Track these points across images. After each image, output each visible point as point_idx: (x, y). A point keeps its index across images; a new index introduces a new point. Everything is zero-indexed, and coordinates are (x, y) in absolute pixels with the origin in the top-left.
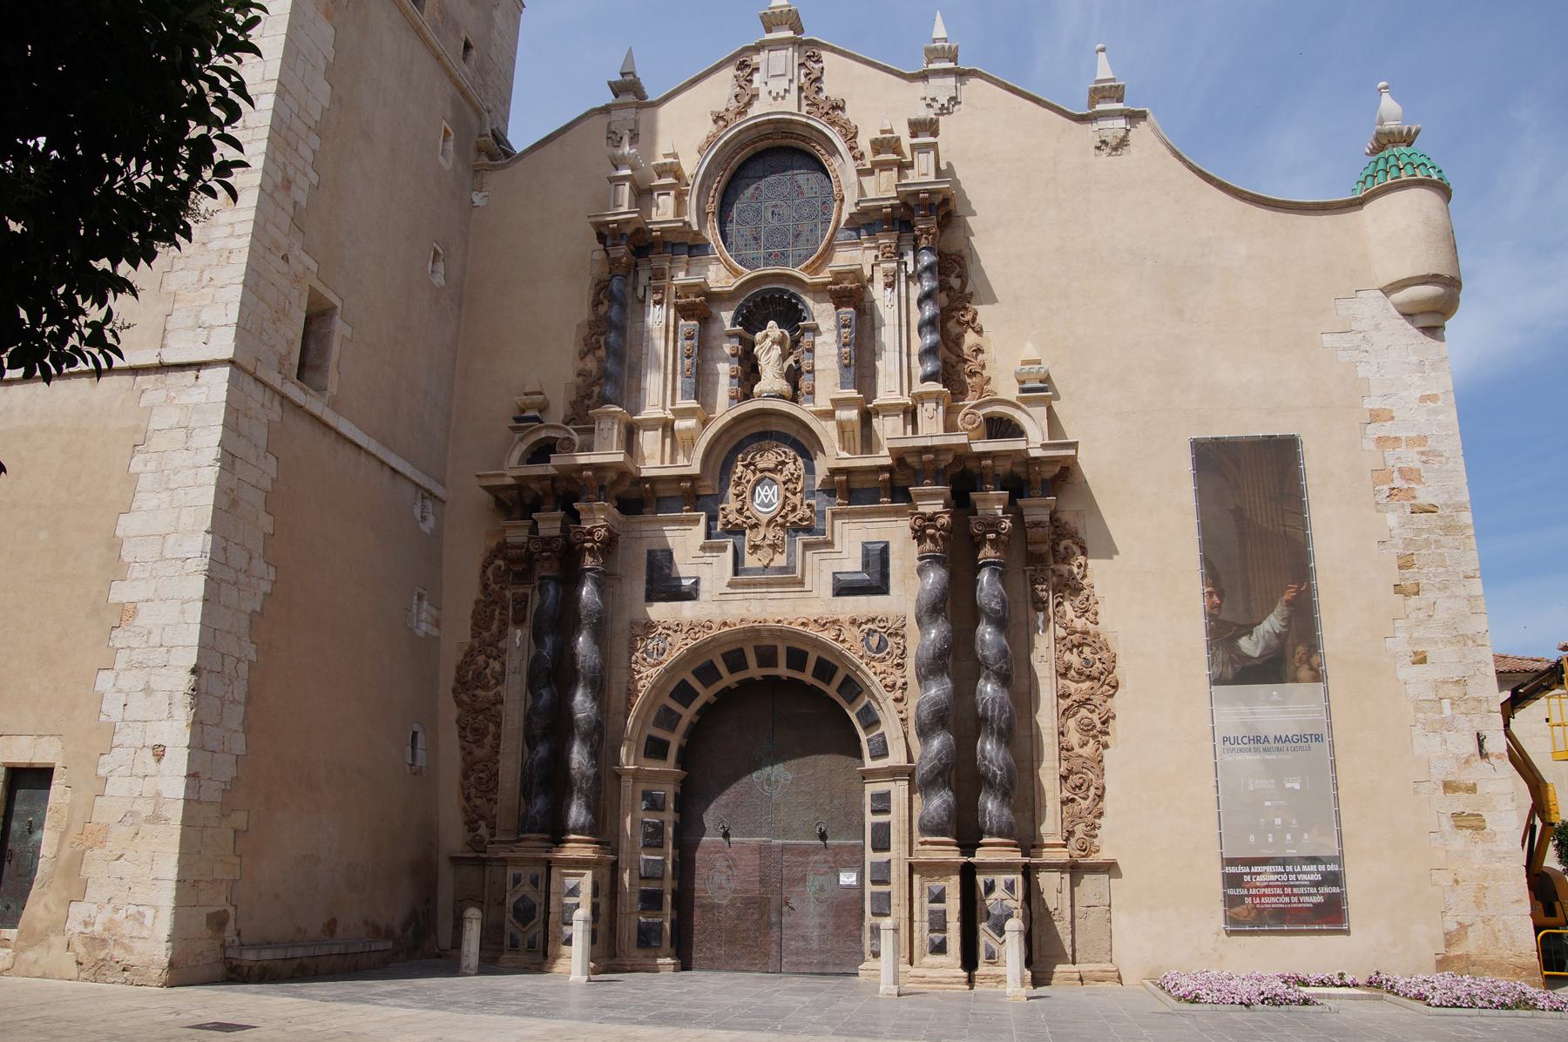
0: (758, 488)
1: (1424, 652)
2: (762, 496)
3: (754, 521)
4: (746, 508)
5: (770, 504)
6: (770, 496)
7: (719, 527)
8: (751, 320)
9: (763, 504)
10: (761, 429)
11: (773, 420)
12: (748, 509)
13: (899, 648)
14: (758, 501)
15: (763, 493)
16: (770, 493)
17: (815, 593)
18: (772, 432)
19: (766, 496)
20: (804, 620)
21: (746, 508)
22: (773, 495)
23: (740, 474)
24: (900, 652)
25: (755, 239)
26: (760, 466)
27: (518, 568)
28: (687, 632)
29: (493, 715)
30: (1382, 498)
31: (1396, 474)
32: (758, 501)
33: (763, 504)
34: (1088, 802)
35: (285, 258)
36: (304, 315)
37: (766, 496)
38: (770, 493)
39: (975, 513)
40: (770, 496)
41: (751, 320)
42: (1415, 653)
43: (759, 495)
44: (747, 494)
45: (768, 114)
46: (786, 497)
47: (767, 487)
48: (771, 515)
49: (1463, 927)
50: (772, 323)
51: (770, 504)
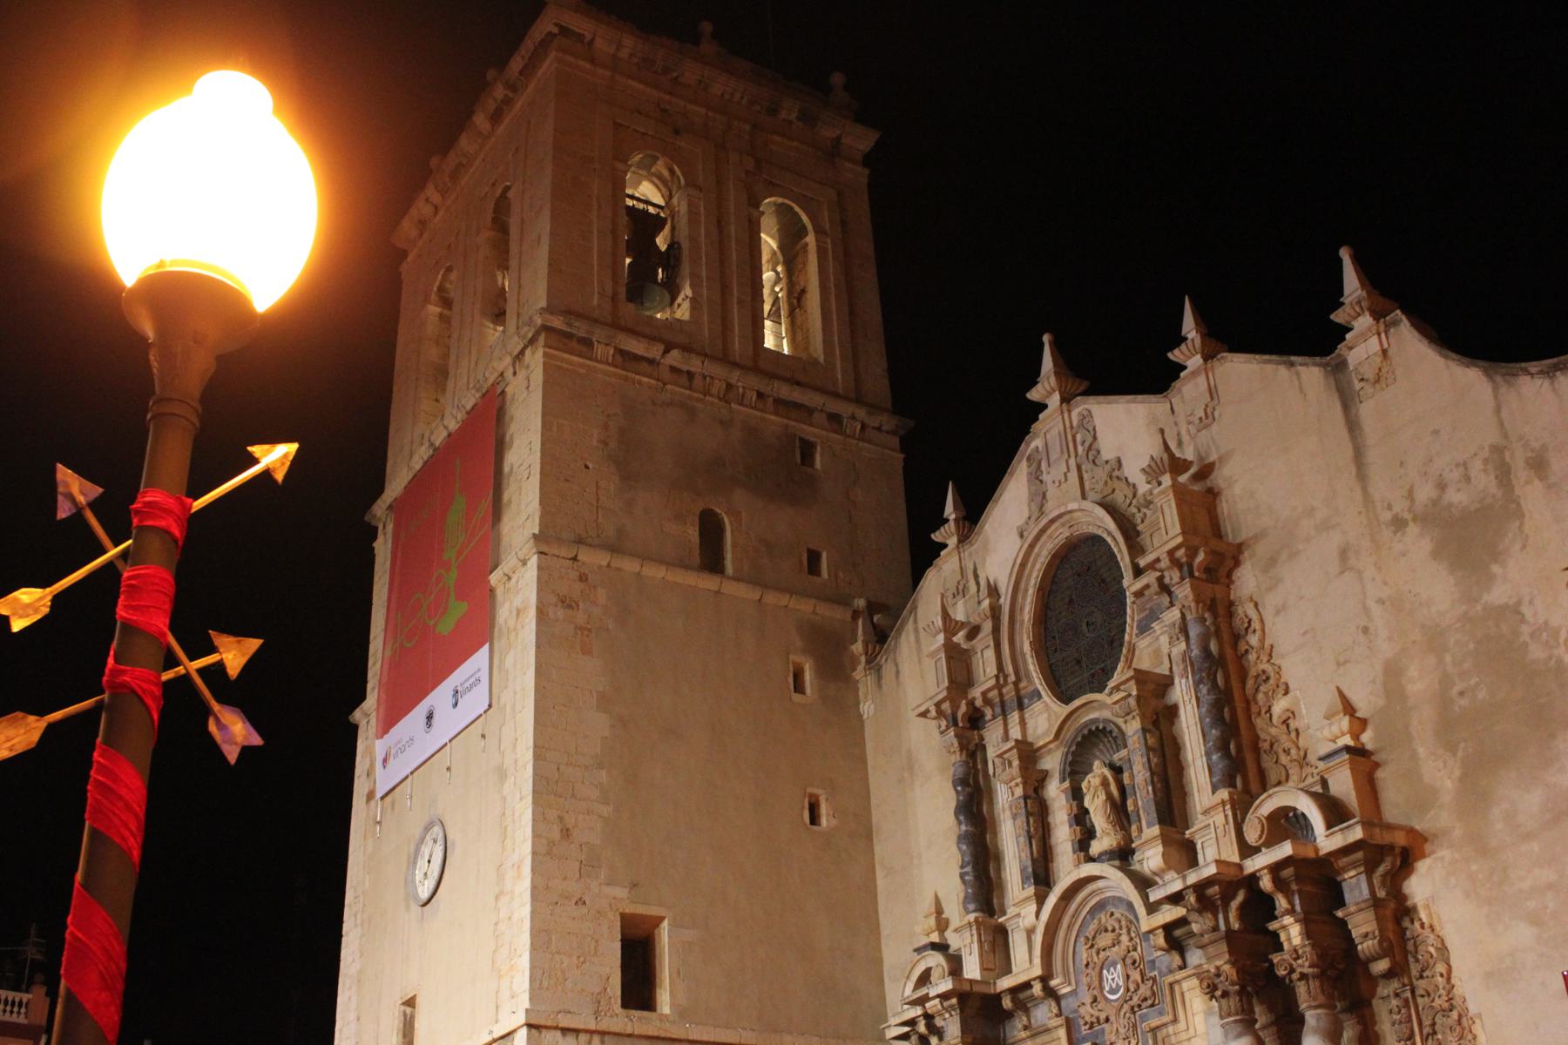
0: (1105, 972)
2: (1110, 980)
6: (1117, 979)
8: (1075, 771)
9: (1112, 991)
14: (1107, 988)
15: (1110, 977)
16: (1115, 975)
19: (1113, 979)
23: (1085, 962)
32: (1107, 988)
35: (581, 902)
36: (618, 945)
37: (1113, 979)
39: (1279, 947)
40: (1117, 979)
41: (1075, 771)
44: (1096, 983)
46: (1128, 976)
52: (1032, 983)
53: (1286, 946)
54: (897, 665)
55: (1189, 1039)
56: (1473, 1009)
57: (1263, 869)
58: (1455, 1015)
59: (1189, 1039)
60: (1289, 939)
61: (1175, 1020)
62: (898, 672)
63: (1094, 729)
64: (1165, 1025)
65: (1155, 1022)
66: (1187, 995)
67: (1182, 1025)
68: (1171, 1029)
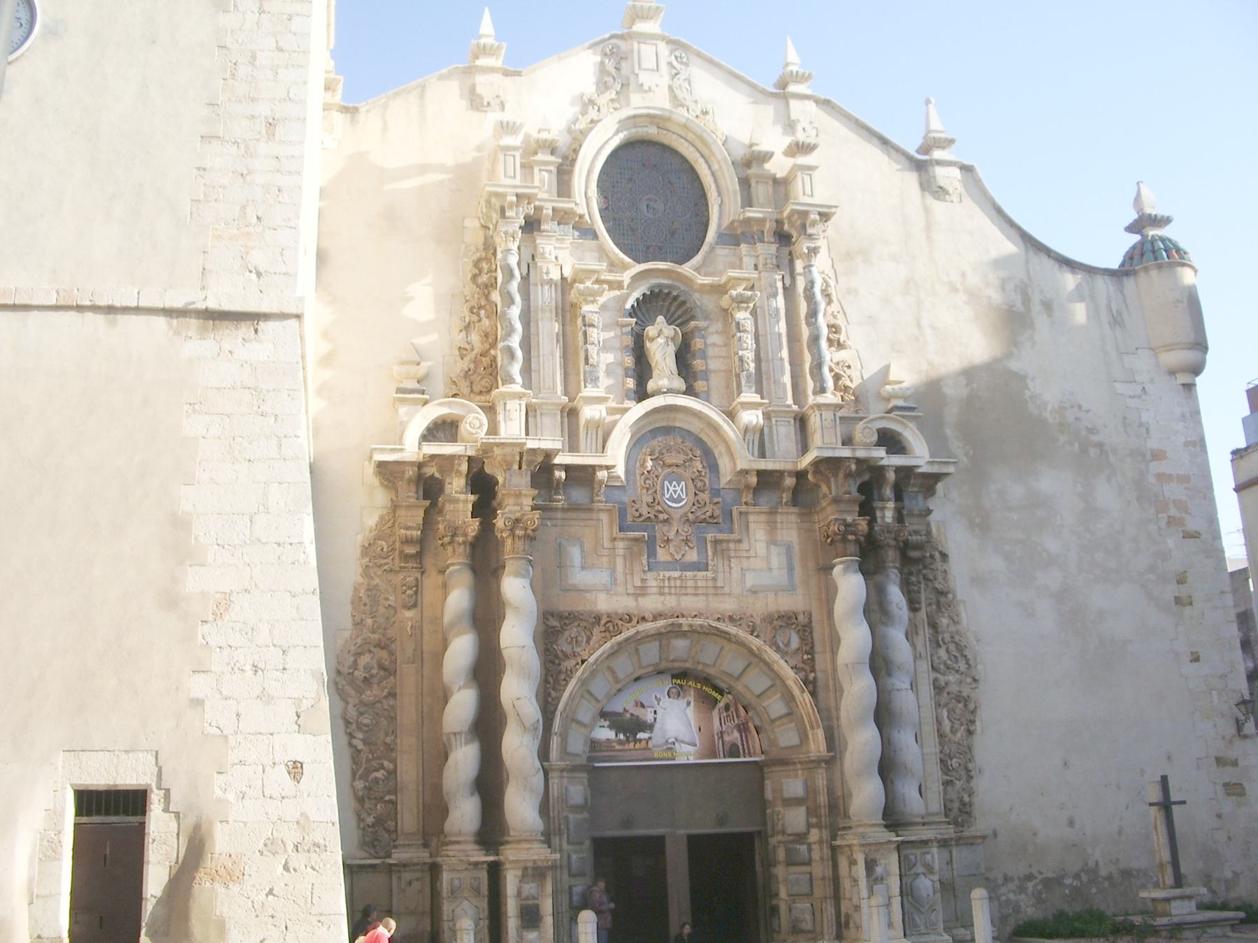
0: (666, 482)
1: (1197, 652)
2: (671, 491)
3: (666, 517)
4: (657, 502)
5: (679, 500)
6: (679, 491)
7: (629, 518)
9: (671, 499)
10: (663, 424)
11: (680, 416)
12: (659, 503)
13: (806, 644)
14: (667, 496)
15: (671, 489)
16: (678, 489)
17: (727, 590)
18: (675, 427)
20: (719, 616)
21: (657, 502)
22: (682, 490)
24: (808, 648)
25: (632, 230)
26: (669, 461)
27: (411, 550)
28: (605, 625)
29: (385, 709)
30: (1163, 523)
31: (1171, 505)
32: (667, 496)
33: (671, 499)
34: (962, 782)
37: (675, 492)
38: (678, 489)
42: (1192, 653)
43: (668, 490)
45: (648, 108)
47: (675, 483)
48: (682, 511)
49: (1236, 874)
50: (661, 319)
51: (679, 500)
52: (597, 468)
53: (879, 520)
54: (385, 123)
55: (748, 558)
56: (960, 596)
57: (892, 466)
58: (950, 596)
59: (748, 558)
60: (883, 517)
61: (740, 541)
62: (385, 129)
63: (666, 291)
64: (728, 541)
65: (720, 536)
66: (752, 526)
67: (745, 546)
68: (732, 546)
